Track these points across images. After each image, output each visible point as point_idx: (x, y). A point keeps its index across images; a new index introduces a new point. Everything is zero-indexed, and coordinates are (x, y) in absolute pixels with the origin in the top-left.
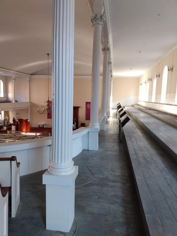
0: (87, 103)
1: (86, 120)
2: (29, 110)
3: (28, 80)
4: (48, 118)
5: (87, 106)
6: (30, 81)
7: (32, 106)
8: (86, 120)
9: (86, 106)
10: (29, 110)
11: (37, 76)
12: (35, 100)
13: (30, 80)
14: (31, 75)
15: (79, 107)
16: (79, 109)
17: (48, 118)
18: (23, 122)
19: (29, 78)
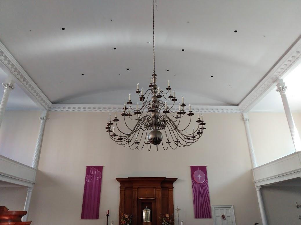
0: (194, 169)
1: (196, 217)
2: (29, 195)
3: (44, 115)
4: (83, 218)
5: (194, 176)
6: (46, 119)
7: (43, 181)
8: (196, 217)
9: (193, 178)
10: (29, 195)
11: (67, 106)
12: (52, 166)
13: (47, 115)
14: (52, 103)
15: (175, 179)
16: (175, 185)
17: (83, 218)
18: (6, 221)
19: (45, 112)
